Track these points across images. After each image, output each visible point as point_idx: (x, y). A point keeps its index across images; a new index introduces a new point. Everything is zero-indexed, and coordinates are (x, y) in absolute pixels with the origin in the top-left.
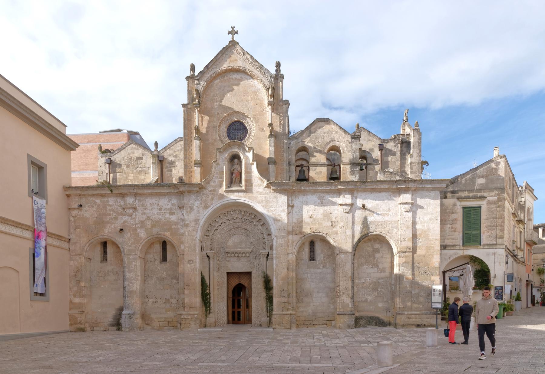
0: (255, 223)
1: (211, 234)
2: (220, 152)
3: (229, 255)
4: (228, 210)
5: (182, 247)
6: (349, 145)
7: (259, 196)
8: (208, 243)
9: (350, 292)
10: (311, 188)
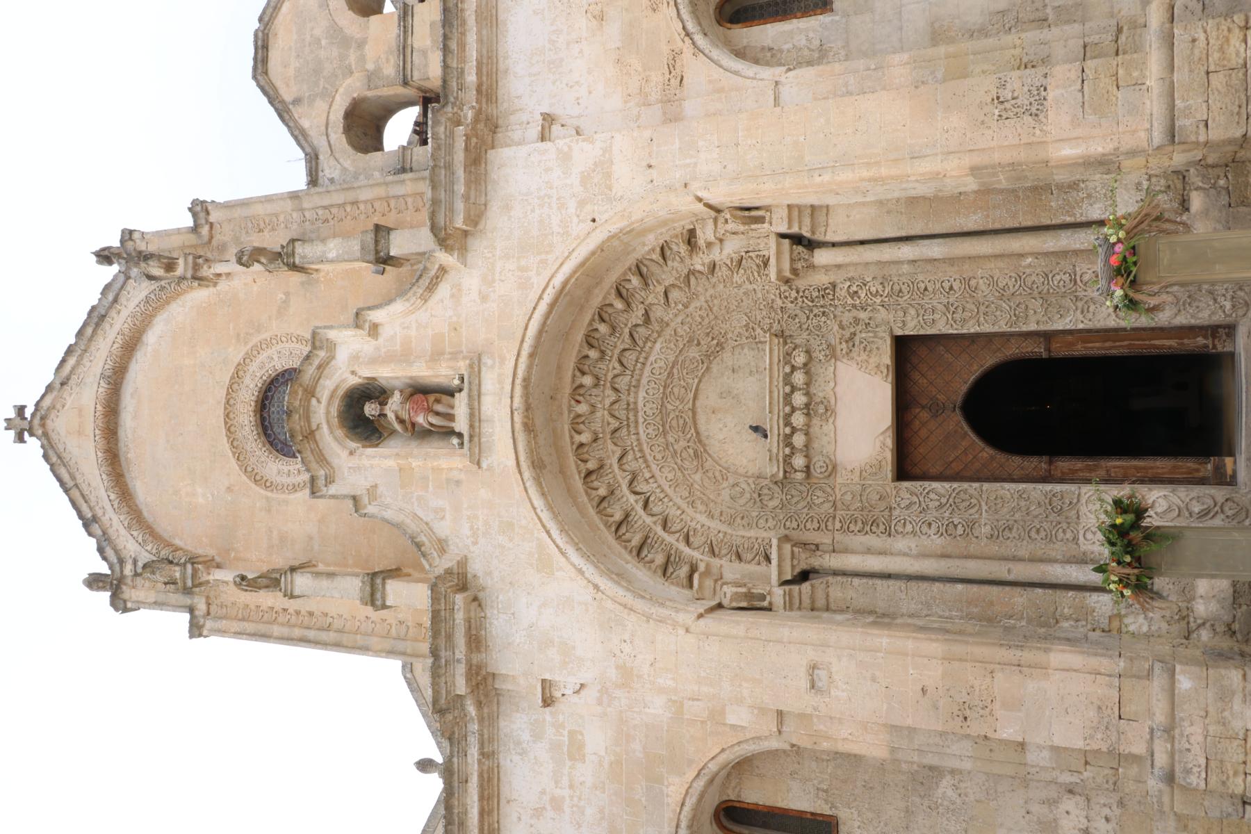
0: (637, 316)
1: (687, 551)
2: (329, 480)
3: (799, 461)
4: (571, 459)
5: (738, 716)
8: (731, 570)
10: (471, 38)
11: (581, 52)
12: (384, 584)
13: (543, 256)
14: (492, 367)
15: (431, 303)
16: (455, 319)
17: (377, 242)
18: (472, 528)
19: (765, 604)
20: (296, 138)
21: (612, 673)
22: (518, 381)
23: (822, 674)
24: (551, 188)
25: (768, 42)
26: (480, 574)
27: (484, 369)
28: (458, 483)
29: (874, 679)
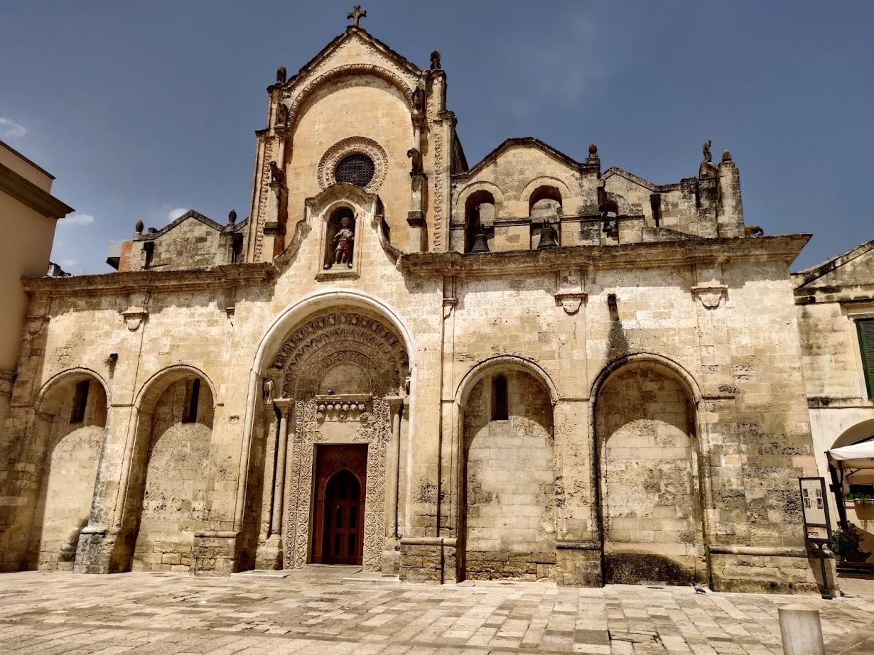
6: (576, 183)
7: (385, 284)
9: (588, 493)
11: (482, 315)
18: (292, 275)
19: (266, 397)
20: (476, 166)
21: (236, 339)
23: (236, 420)
25: (484, 394)
28: (310, 268)
29: (234, 440)
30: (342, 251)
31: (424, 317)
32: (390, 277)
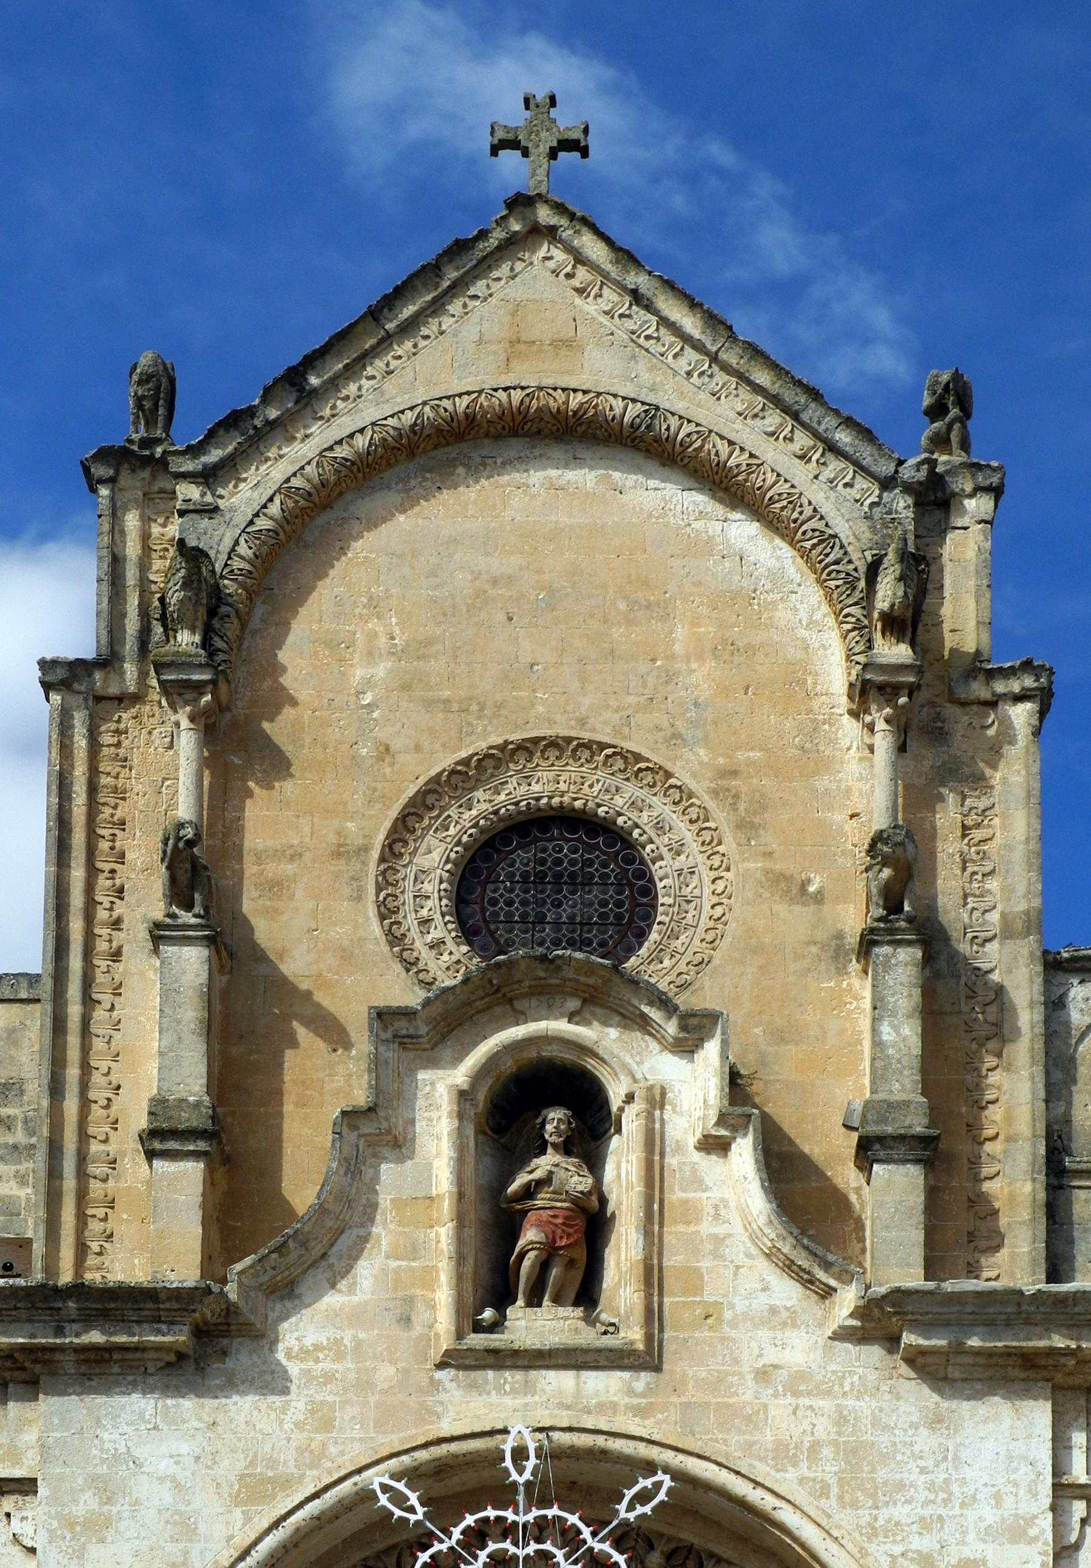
7: (779, 1409)
12: (196, 1155)
13: (835, 1491)
14: (631, 1392)
15: (763, 1266)
16: (728, 1315)
17: (902, 1138)
18: (318, 1347)
22: (600, 1441)
24: (963, 1505)
26: (229, 1363)
27: (626, 1375)
28: (406, 1321)
30: (549, 1255)
31: (967, 1552)
32: (801, 1376)
